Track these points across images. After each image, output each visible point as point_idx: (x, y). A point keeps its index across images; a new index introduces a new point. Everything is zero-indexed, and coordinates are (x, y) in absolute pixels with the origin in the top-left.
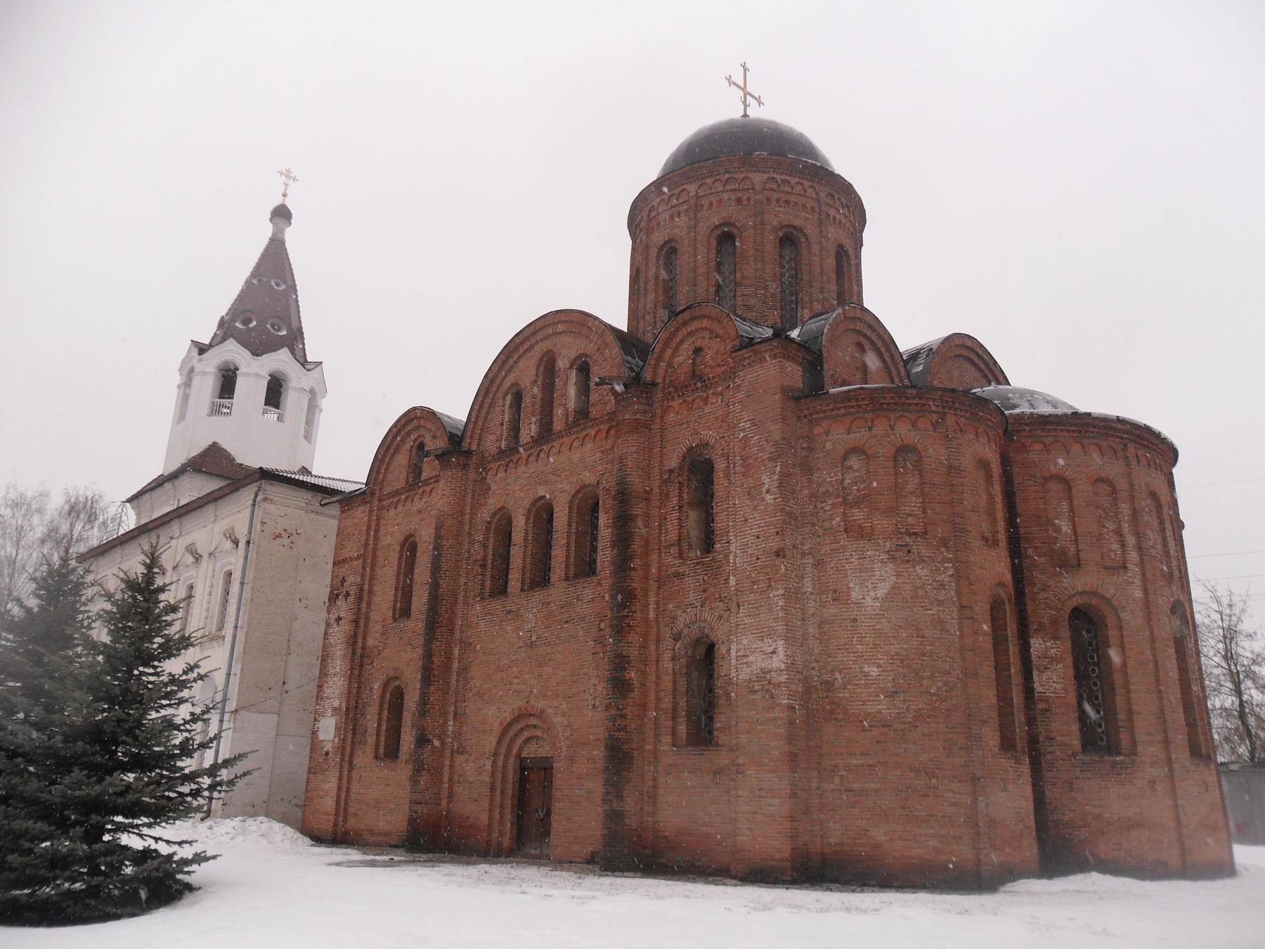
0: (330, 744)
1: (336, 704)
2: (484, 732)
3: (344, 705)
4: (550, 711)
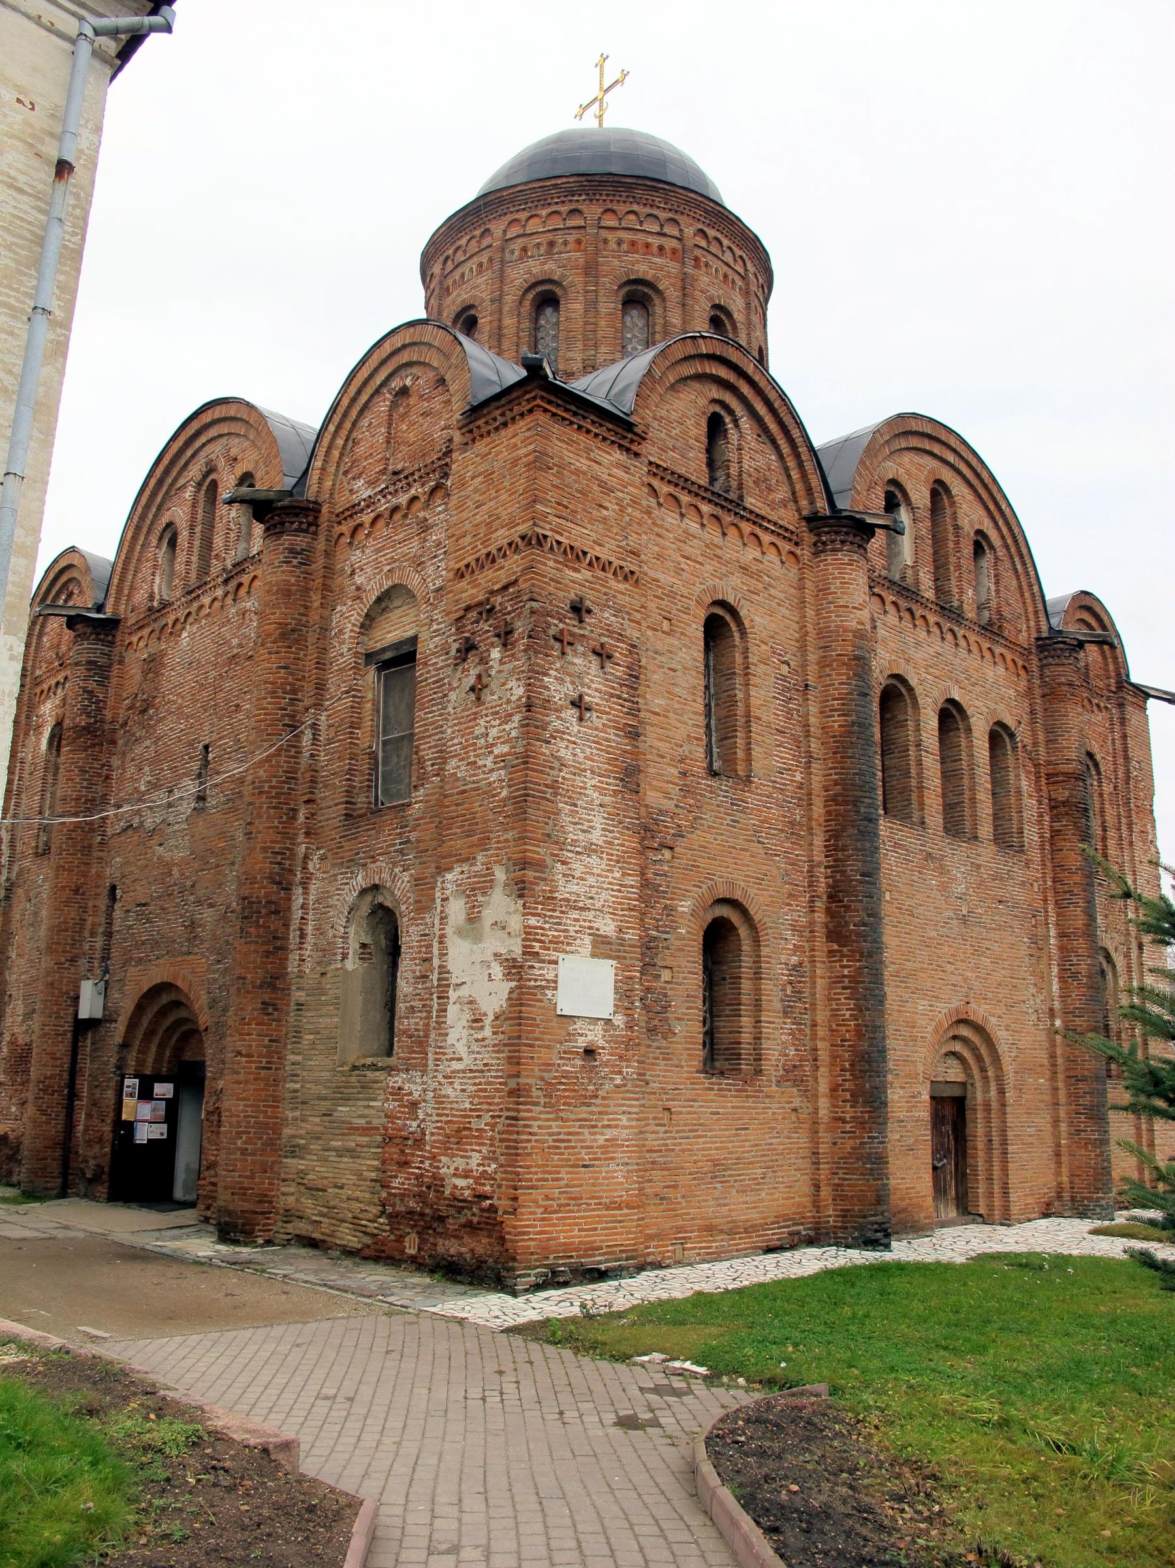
0: (599, 1027)
1: (608, 927)
2: (914, 1039)
3: (631, 936)
4: (994, 1020)
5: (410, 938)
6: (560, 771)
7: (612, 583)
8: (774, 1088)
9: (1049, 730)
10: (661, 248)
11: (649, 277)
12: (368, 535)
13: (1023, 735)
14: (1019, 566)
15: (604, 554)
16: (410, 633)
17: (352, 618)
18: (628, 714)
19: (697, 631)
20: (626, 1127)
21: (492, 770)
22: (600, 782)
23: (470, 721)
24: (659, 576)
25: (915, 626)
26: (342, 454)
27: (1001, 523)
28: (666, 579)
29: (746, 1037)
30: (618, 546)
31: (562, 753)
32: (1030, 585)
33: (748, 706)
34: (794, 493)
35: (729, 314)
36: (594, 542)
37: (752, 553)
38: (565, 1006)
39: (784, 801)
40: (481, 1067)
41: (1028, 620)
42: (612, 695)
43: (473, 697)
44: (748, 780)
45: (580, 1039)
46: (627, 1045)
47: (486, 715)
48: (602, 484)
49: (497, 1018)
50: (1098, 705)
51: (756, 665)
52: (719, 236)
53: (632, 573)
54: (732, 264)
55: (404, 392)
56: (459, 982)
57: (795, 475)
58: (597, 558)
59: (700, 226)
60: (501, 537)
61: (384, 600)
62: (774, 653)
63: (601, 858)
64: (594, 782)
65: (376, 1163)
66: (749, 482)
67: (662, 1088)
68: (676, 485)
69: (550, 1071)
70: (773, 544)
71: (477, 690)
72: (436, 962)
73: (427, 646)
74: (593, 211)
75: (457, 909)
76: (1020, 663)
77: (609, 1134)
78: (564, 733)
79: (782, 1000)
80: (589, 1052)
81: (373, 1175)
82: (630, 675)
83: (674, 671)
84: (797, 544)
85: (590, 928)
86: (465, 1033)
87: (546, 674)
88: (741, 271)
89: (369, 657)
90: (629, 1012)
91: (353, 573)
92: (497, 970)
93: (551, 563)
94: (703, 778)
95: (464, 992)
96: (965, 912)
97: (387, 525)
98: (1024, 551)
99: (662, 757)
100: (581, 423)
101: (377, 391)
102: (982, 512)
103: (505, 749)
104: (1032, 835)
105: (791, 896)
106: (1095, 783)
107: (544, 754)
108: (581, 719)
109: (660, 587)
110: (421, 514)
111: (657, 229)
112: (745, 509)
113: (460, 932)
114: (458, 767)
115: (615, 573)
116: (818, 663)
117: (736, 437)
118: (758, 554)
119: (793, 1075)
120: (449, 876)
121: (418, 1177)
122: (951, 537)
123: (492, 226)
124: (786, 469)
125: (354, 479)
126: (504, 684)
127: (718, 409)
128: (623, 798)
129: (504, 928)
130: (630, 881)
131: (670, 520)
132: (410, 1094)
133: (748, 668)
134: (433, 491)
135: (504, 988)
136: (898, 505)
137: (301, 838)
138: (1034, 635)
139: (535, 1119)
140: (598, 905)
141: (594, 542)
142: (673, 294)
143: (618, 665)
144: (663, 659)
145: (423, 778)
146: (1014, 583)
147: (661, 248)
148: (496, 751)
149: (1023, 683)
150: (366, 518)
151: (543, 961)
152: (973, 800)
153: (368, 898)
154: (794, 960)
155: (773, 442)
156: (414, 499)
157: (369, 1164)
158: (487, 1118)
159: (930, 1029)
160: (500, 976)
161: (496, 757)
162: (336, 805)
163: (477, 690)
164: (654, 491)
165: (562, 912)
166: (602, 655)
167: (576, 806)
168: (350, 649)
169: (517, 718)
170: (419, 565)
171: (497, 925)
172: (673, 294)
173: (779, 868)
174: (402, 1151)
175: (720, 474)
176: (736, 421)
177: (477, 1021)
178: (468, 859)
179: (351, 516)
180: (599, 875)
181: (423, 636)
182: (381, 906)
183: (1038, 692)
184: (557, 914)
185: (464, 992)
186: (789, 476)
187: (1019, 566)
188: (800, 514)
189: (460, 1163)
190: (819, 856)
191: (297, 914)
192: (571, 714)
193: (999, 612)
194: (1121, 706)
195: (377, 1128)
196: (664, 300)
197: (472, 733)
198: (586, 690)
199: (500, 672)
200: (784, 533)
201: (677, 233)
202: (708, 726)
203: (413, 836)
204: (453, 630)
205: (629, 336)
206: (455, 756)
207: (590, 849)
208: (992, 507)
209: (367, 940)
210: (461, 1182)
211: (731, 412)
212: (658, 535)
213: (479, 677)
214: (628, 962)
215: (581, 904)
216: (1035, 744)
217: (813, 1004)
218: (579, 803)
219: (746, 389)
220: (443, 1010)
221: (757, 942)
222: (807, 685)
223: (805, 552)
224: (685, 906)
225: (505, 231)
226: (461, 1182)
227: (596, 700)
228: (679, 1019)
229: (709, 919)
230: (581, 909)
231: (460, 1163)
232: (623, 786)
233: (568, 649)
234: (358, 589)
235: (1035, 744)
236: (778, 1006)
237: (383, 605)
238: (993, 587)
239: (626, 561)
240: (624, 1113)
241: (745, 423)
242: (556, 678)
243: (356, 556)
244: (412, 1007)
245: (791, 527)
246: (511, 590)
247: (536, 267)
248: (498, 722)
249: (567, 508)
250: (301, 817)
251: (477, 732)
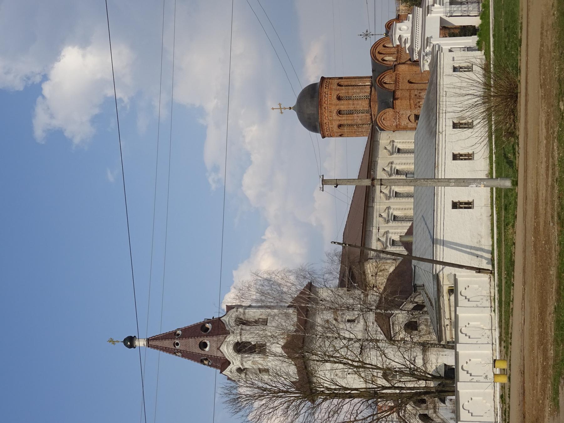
11: (336, 96)
16: (414, 116)
27: (380, 43)
55: (384, 119)
60: (408, 103)
74: (325, 105)
123: (325, 122)
142: (338, 92)
166: (420, 93)
172: (338, 92)
208: (378, 44)
219: (380, 80)
243: (402, 124)
247: (334, 114)
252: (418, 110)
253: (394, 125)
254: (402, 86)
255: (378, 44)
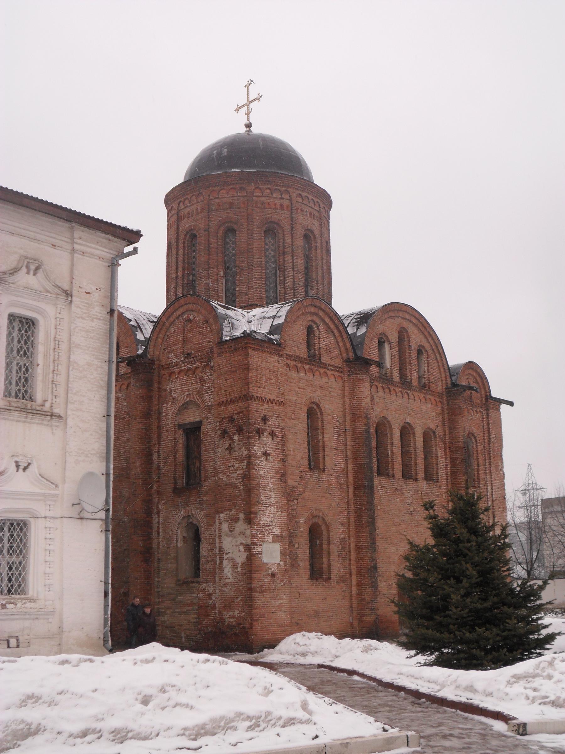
0: (276, 566)
1: (277, 531)
3: (285, 533)
5: (205, 536)
6: (260, 479)
7: (275, 407)
8: (336, 584)
9: (450, 428)
10: (281, 205)
12: (177, 378)
13: (439, 431)
14: (438, 358)
15: (272, 397)
16: (198, 420)
17: (172, 410)
18: (281, 455)
19: (304, 416)
20: (285, 599)
21: (236, 479)
22: (273, 481)
23: (227, 460)
24: (291, 398)
25: (390, 394)
26: (163, 341)
27: (430, 339)
28: (293, 398)
29: (325, 566)
30: (277, 393)
31: (261, 473)
32: (443, 365)
33: (324, 441)
34: (340, 351)
35: (312, 232)
36: (269, 393)
37: (325, 380)
38: (265, 559)
39: (338, 476)
40: (237, 581)
41: (442, 380)
42: (276, 449)
43: (228, 452)
44: (324, 471)
45: (270, 570)
46: (285, 572)
47: (233, 459)
48: (271, 371)
49: (242, 564)
50: (476, 411)
51: (326, 425)
52: (307, 195)
53: (282, 402)
54: (313, 207)
55: (189, 321)
56: (227, 552)
57: (341, 344)
58: (270, 399)
59: (299, 192)
61: (186, 406)
62: (333, 418)
63: (274, 508)
64: (271, 481)
65: (196, 616)
66: (322, 351)
67: (296, 586)
68: (296, 361)
69: (261, 582)
70: (333, 375)
71: (230, 448)
72: (217, 545)
73: (207, 427)
75: (225, 527)
76: (438, 400)
77: (280, 602)
78: (261, 465)
79: (338, 552)
80: (273, 575)
81: (195, 620)
82: (282, 440)
83: (296, 433)
84: (341, 372)
85: (272, 532)
86: (230, 570)
87: (254, 446)
88: (317, 208)
89: (180, 426)
90: (285, 560)
91: (171, 391)
92: (241, 548)
93: (255, 405)
94: (307, 472)
95: (230, 555)
96: (411, 510)
97: (186, 375)
98: (441, 351)
99: (294, 466)
100: (263, 349)
101: (178, 318)
102: (421, 336)
103: (241, 472)
104: (442, 474)
105: (341, 512)
106: (475, 446)
107: (255, 474)
108: (266, 459)
109: (290, 402)
110: (201, 374)
111: (280, 196)
112: (321, 363)
113: (227, 535)
114: (223, 476)
115: (276, 404)
116: (350, 420)
117: (318, 333)
118: (326, 380)
119: (342, 579)
120: (221, 515)
121: (213, 620)
122: (407, 351)
124: (338, 343)
125: (169, 352)
126: (240, 449)
127: (311, 323)
128: (281, 485)
129: (244, 534)
130: (284, 514)
131: (294, 375)
132: (209, 591)
133: (323, 426)
134: (205, 366)
135: (245, 555)
136: (384, 342)
137: (155, 496)
138: (445, 386)
139: (257, 597)
140: (274, 524)
141: (269, 393)
143: (278, 437)
144: (293, 430)
145: (207, 478)
146: (436, 365)
147: (281, 205)
148: (238, 473)
149: (440, 409)
150: (177, 370)
151: (258, 545)
152: (416, 463)
153: (186, 520)
154: (342, 536)
155: (332, 332)
156: (197, 368)
157: (192, 617)
158: (240, 598)
159: (396, 558)
160: (243, 550)
161: (238, 474)
162: (170, 483)
163: (230, 448)
164: (288, 365)
165: (263, 528)
166: (273, 434)
167: (266, 490)
168: (171, 423)
169: (245, 462)
170: (200, 394)
171: (242, 534)
172: (287, 228)
173: (336, 502)
174: (206, 611)
175: (312, 348)
176: (318, 327)
177: (235, 566)
178: (229, 509)
179: (168, 368)
180: (274, 514)
181: (204, 422)
182: (191, 523)
183: (446, 411)
184: (261, 529)
185: (230, 555)
186: (338, 345)
187: (438, 358)
188: (343, 360)
189: (231, 613)
190: (351, 495)
191: (155, 525)
192: (263, 459)
193: (429, 379)
194: (487, 410)
195: (195, 604)
196: (283, 231)
197: (228, 465)
198: (268, 449)
199: (238, 444)
200: (336, 368)
201: (289, 198)
202: (309, 449)
203: (205, 499)
204: (218, 424)
205: (267, 247)
206: (222, 472)
207: (271, 505)
208: (426, 333)
209: (186, 535)
210: (232, 620)
211: (316, 323)
212: (290, 382)
213: (230, 445)
214: (284, 543)
215: (268, 524)
216: (445, 435)
217: (350, 552)
218: (267, 489)
219: (321, 313)
220: (221, 563)
221: (328, 531)
222: (346, 429)
223: (345, 375)
224: (302, 520)
225: (209, 196)
226: (232, 620)
227: (271, 452)
228: (301, 561)
229: (311, 522)
230: (269, 526)
231: (231, 613)
232: (281, 481)
233: (262, 436)
234: (174, 398)
235: (445, 435)
236: (337, 554)
237: (185, 406)
238: (426, 369)
239: (279, 397)
240: (284, 594)
241: (321, 327)
242: (258, 446)
243: (172, 385)
244: (208, 560)
245: (340, 366)
246: (241, 414)
248: (238, 462)
249: (259, 383)
250: (155, 487)
251: (230, 465)
252: (214, 430)
253: (172, 355)
254: (300, 378)
255: (426, 333)
